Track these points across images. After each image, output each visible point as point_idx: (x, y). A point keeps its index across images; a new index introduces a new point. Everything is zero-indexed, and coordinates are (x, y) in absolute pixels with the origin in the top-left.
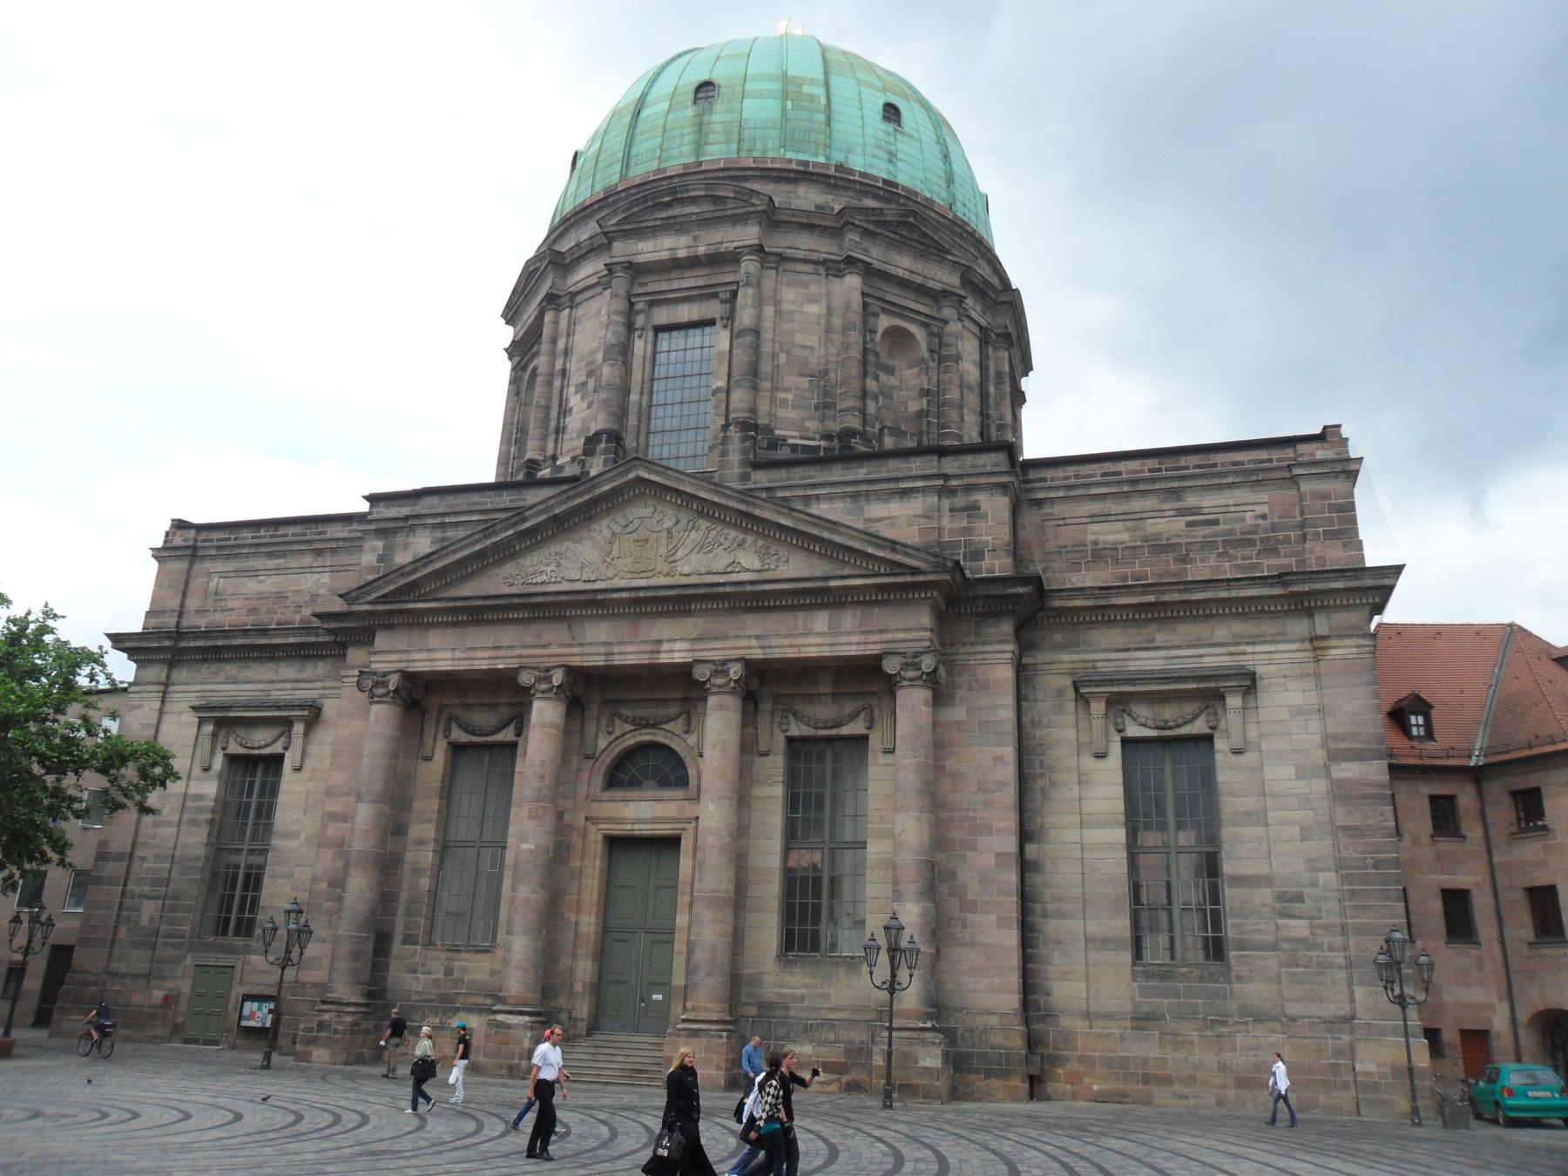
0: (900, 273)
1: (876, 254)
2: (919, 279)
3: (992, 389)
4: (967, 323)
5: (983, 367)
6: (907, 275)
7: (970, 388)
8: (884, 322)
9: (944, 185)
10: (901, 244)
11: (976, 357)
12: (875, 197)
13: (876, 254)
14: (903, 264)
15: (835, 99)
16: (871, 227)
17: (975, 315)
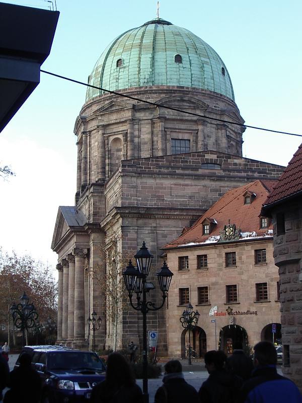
0: (113, 122)
1: (106, 120)
2: (118, 121)
3: (155, 139)
4: (143, 122)
5: (152, 133)
6: (115, 121)
7: (145, 143)
8: (111, 138)
9: (137, 76)
10: (112, 112)
11: (150, 130)
12: (107, 100)
13: (106, 120)
14: (114, 118)
15: (105, 68)
16: (101, 114)
17: (145, 118)
